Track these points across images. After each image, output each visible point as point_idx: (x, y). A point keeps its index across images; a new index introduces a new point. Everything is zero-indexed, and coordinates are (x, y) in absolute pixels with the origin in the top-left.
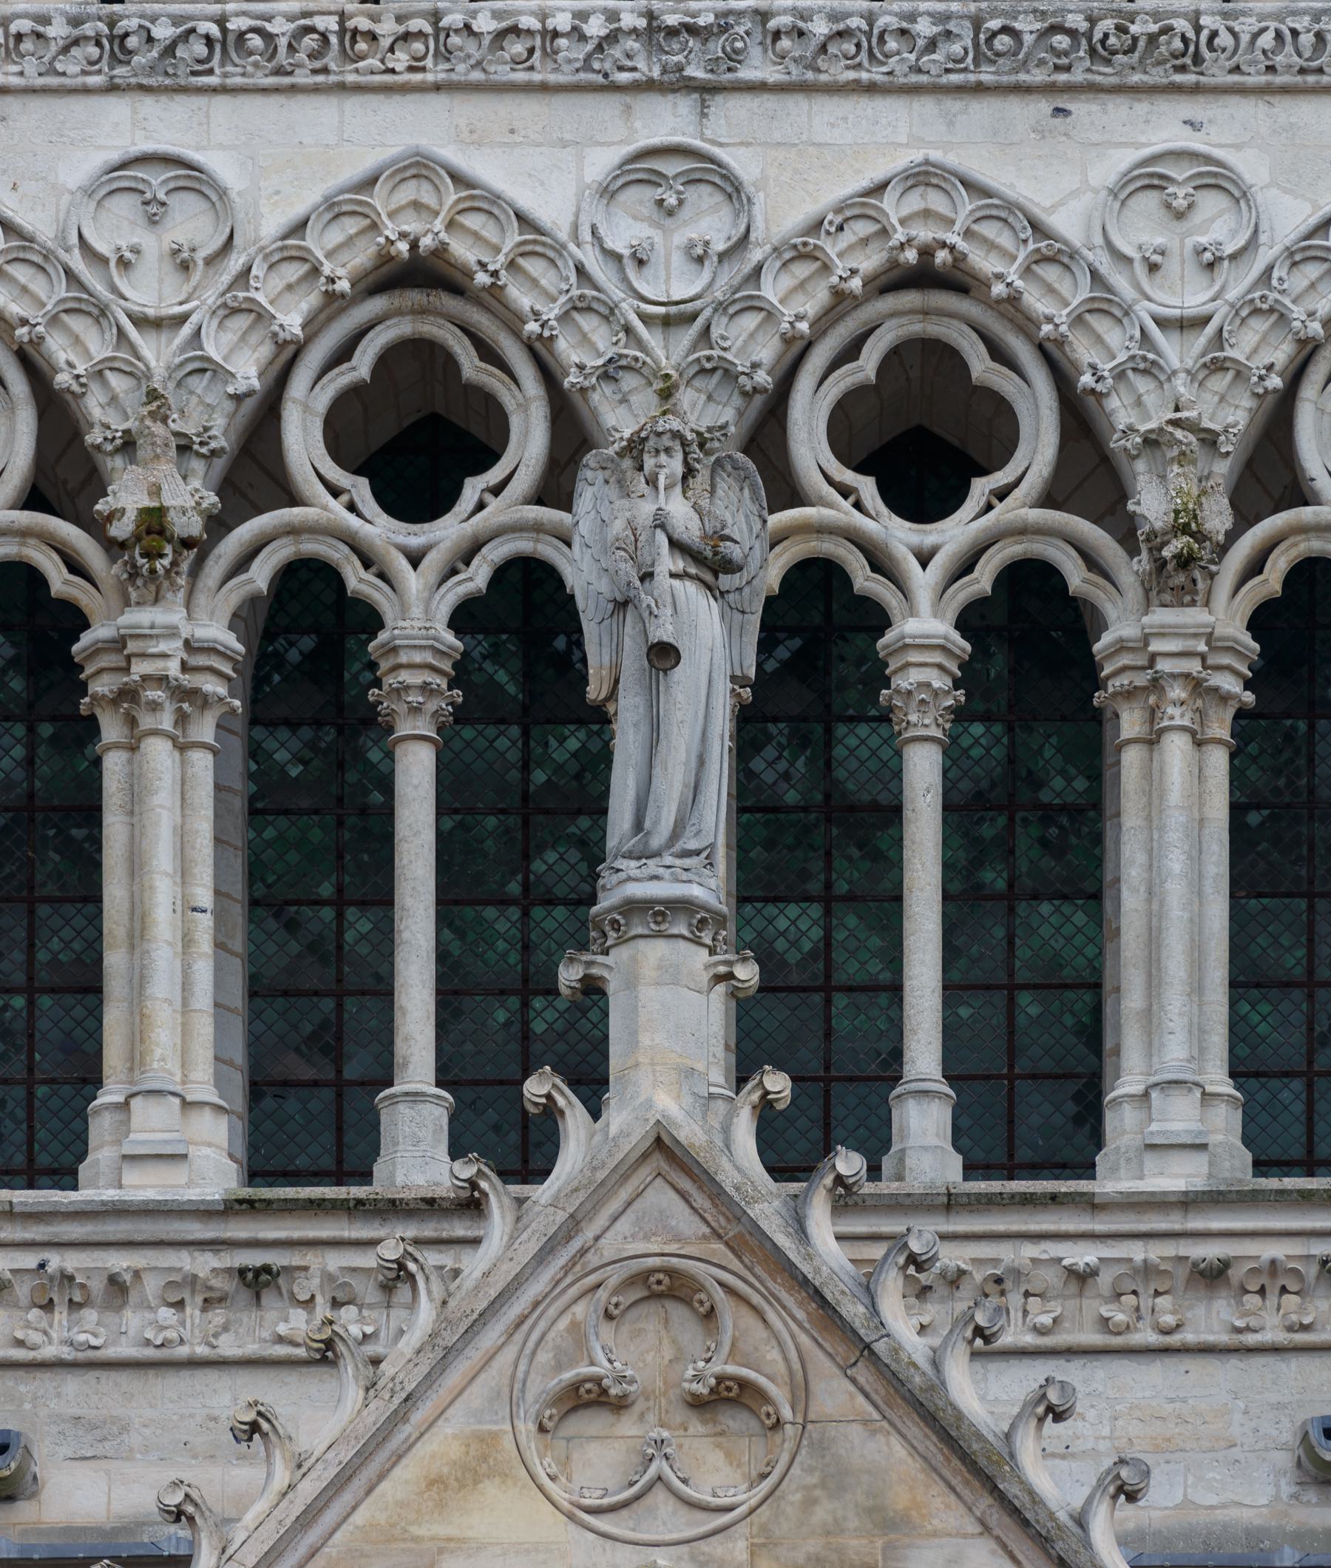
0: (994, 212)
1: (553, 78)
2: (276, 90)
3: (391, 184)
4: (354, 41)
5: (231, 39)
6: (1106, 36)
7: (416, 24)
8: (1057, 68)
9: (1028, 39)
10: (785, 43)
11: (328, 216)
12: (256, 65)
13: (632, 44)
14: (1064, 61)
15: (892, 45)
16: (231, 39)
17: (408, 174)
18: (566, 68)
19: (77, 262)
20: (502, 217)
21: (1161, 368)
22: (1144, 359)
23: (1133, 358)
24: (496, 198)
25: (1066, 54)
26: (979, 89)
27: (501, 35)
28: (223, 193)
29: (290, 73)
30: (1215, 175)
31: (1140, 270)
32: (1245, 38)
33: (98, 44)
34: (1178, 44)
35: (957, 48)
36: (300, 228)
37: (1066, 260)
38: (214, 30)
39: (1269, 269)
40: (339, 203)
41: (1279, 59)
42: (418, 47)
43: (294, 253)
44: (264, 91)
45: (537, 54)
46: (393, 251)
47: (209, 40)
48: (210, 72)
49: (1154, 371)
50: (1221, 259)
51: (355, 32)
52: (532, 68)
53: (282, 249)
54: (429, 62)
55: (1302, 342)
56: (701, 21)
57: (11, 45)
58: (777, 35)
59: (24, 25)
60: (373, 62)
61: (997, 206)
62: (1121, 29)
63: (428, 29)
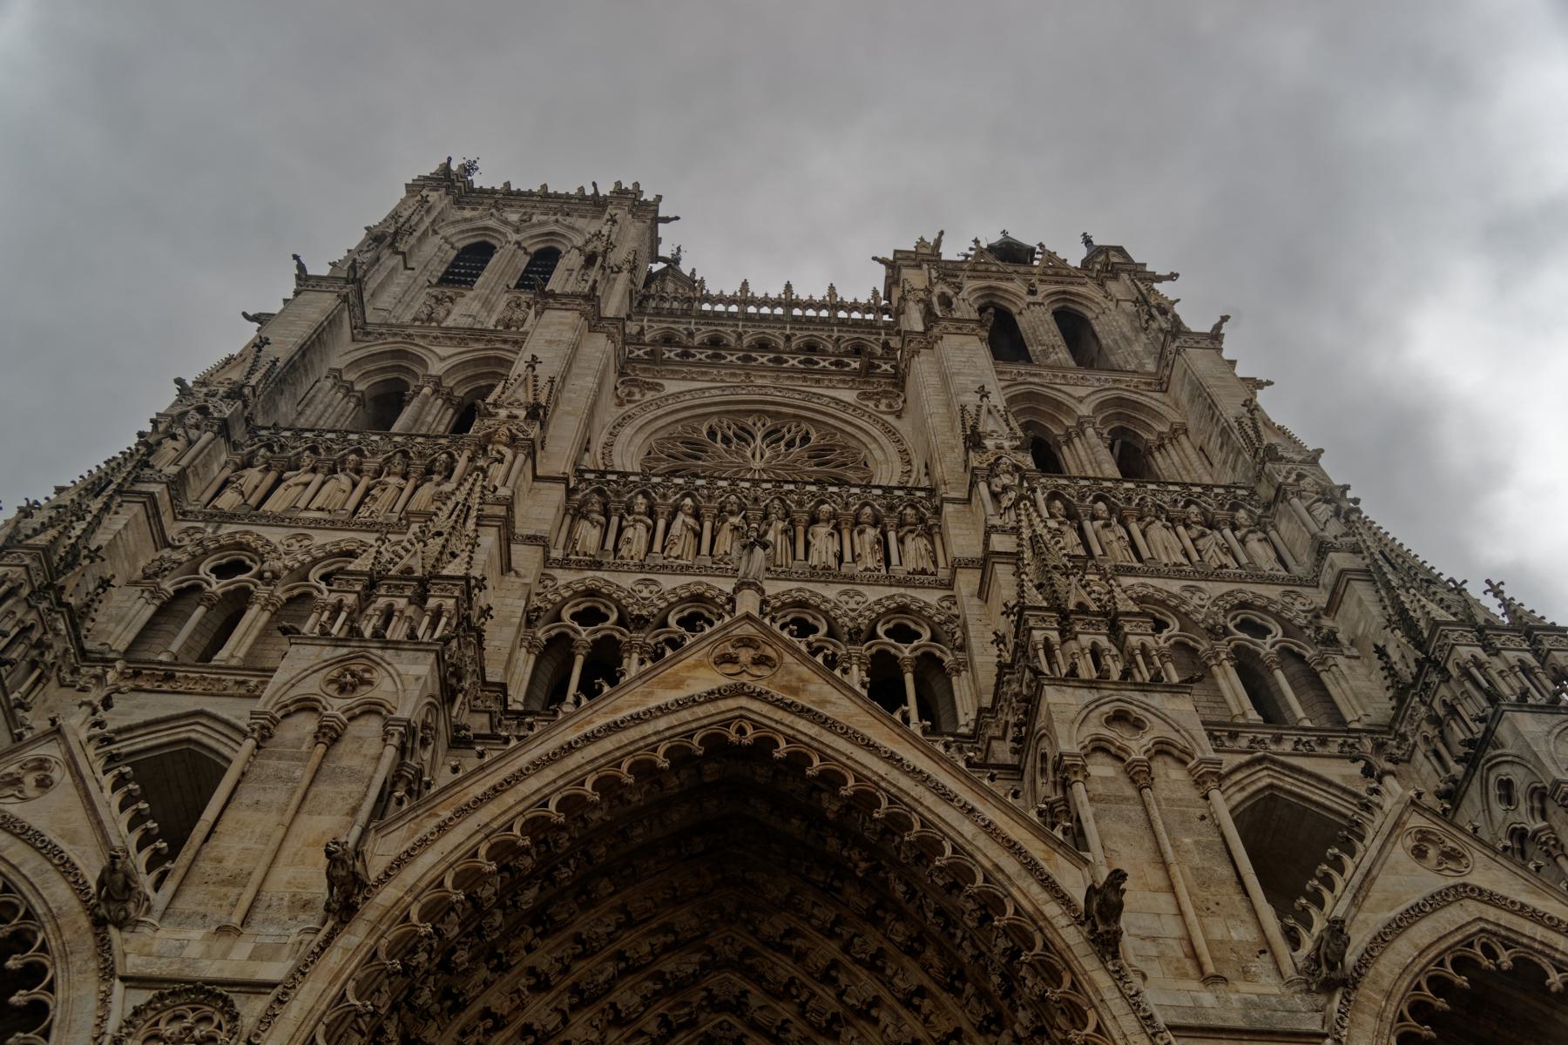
55: (878, 614)
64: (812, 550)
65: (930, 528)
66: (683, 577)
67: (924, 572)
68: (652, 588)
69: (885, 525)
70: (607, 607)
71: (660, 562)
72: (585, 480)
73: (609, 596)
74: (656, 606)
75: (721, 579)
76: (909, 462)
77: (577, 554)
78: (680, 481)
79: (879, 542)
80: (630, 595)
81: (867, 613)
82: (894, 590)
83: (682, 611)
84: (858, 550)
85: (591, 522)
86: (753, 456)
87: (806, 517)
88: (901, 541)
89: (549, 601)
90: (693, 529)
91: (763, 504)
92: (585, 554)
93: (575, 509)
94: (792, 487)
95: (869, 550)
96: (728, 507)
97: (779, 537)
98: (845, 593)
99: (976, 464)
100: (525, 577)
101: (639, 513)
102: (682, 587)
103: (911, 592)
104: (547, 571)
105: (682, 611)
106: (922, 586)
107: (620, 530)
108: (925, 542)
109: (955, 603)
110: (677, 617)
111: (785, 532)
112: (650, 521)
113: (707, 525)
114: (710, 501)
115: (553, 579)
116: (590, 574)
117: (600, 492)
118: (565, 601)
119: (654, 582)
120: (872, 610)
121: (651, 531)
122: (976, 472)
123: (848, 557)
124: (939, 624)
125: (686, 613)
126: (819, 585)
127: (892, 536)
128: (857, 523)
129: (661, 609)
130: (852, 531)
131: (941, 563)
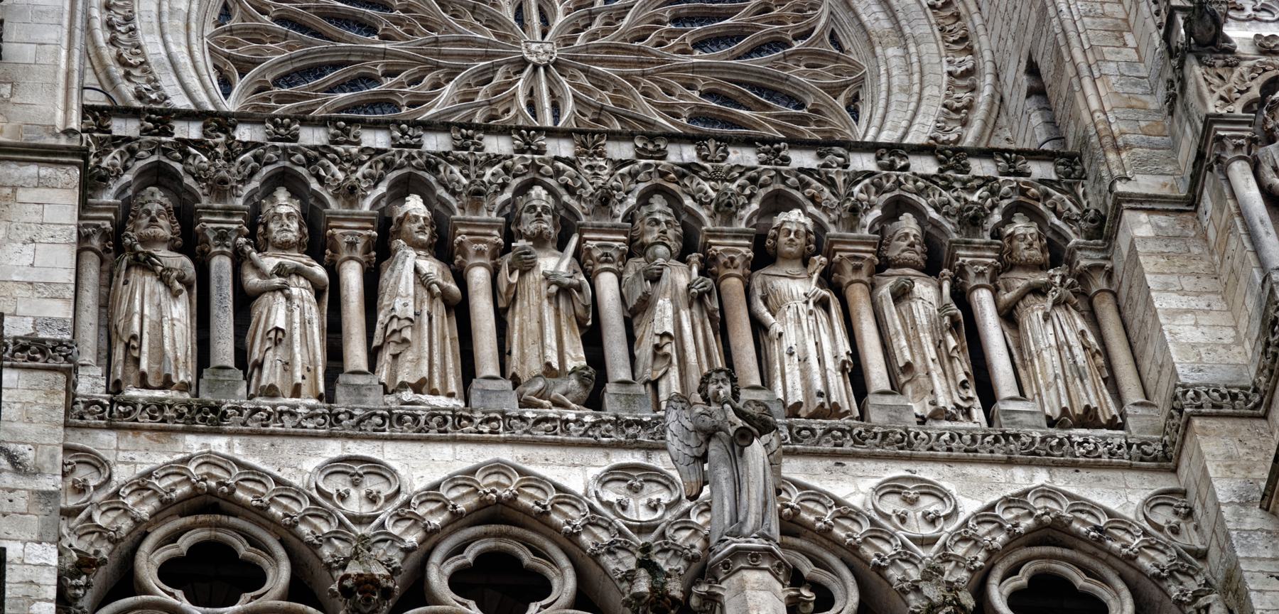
0: (811, 497)
2: (419, 440)
3: (484, 474)
4: (459, 421)
5: (395, 417)
6: (860, 432)
7: (492, 415)
8: (836, 445)
9: (819, 432)
11: (451, 485)
12: (408, 427)
14: (839, 441)
16: (395, 417)
17: (493, 471)
19: (315, 494)
20: (546, 488)
21: (916, 558)
22: (906, 553)
23: (899, 553)
25: (839, 438)
27: (538, 422)
28: (393, 472)
29: (427, 432)
30: (928, 487)
32: (934, 436)
33: (324, 418)
34: (899, 436)
36: (436, 487)
37: (854, 516)
38: (385, 413)
39: (966, 522)
40: (457, 479)
42: (495, 424)
43: (433, 497)
44: (413, 440)
45: (558, 428)
46: (488, 497)
47: (383, 417)
48: (384, 430)
49: (912, 560)
50: (939, 517)
51: (461, 417)
52: (556, 434)
53: (427, 495)
54: (501, 430)
55: (991, 552)
56: (645, 419)
57: (277, 416)
59: (285, 408)
61: (813, 494)
62: (867, 431)
63: (499, 417)
64: (776, 351)
65: (1083, 277)
66: (446, 451)
67: (1089, 418)
68: (373, 484)
69: (962, 271)
70: (254, 542)
71: (376, 401)
72: (117, 141)
73: (260, 514)
74: (395, 539)
75: (553, 453)
76: (964, 42)
77: (143, 383)
78: (377, 139)
79: (954, 326)
80: (319, 511)
81: (960, 550)
82: (1021, 479)
83: (459, 550)
84: (904, 354)
85: (163, 279)
86: (519, 14)
87: (745, 250)
88: (1009, 316)
89: (101, 532)
90: (445, 296)
91: (621, 210)
92: (167, 384)
93: (105, 235)
94: (689, 154)
95: (931, 353)
96: (529, 226)
97: (685, 315)
99: (1213, 106)
100: (38, 472)
101: (285, 246)
102: (453, 481)
103: (1064, 482)
104: (79, 440)
105: (459, 550)
106: (1091, 462)
107: (245, 302)
108: (1081, 324)
109: (1190, 514)
110: (449, 568)
111: (697, 299)
112: (320, 271)
113: (479, 277)
114: (476, 207)
115: (98, 464)
116: (193, 444)
117: (159, 176)
118: (141, 531)
119: (377, 468)
120: (976, 542)
121: (330, 295)
122: (1222, 131)
123: (877, 376)
124: (1157, 578)
125: (469, 556)
126: (819, 465)
127: (984, 302)
128: (883, 266)
129: (407, 551)
130: (872, 287)
131: (1132, 393)
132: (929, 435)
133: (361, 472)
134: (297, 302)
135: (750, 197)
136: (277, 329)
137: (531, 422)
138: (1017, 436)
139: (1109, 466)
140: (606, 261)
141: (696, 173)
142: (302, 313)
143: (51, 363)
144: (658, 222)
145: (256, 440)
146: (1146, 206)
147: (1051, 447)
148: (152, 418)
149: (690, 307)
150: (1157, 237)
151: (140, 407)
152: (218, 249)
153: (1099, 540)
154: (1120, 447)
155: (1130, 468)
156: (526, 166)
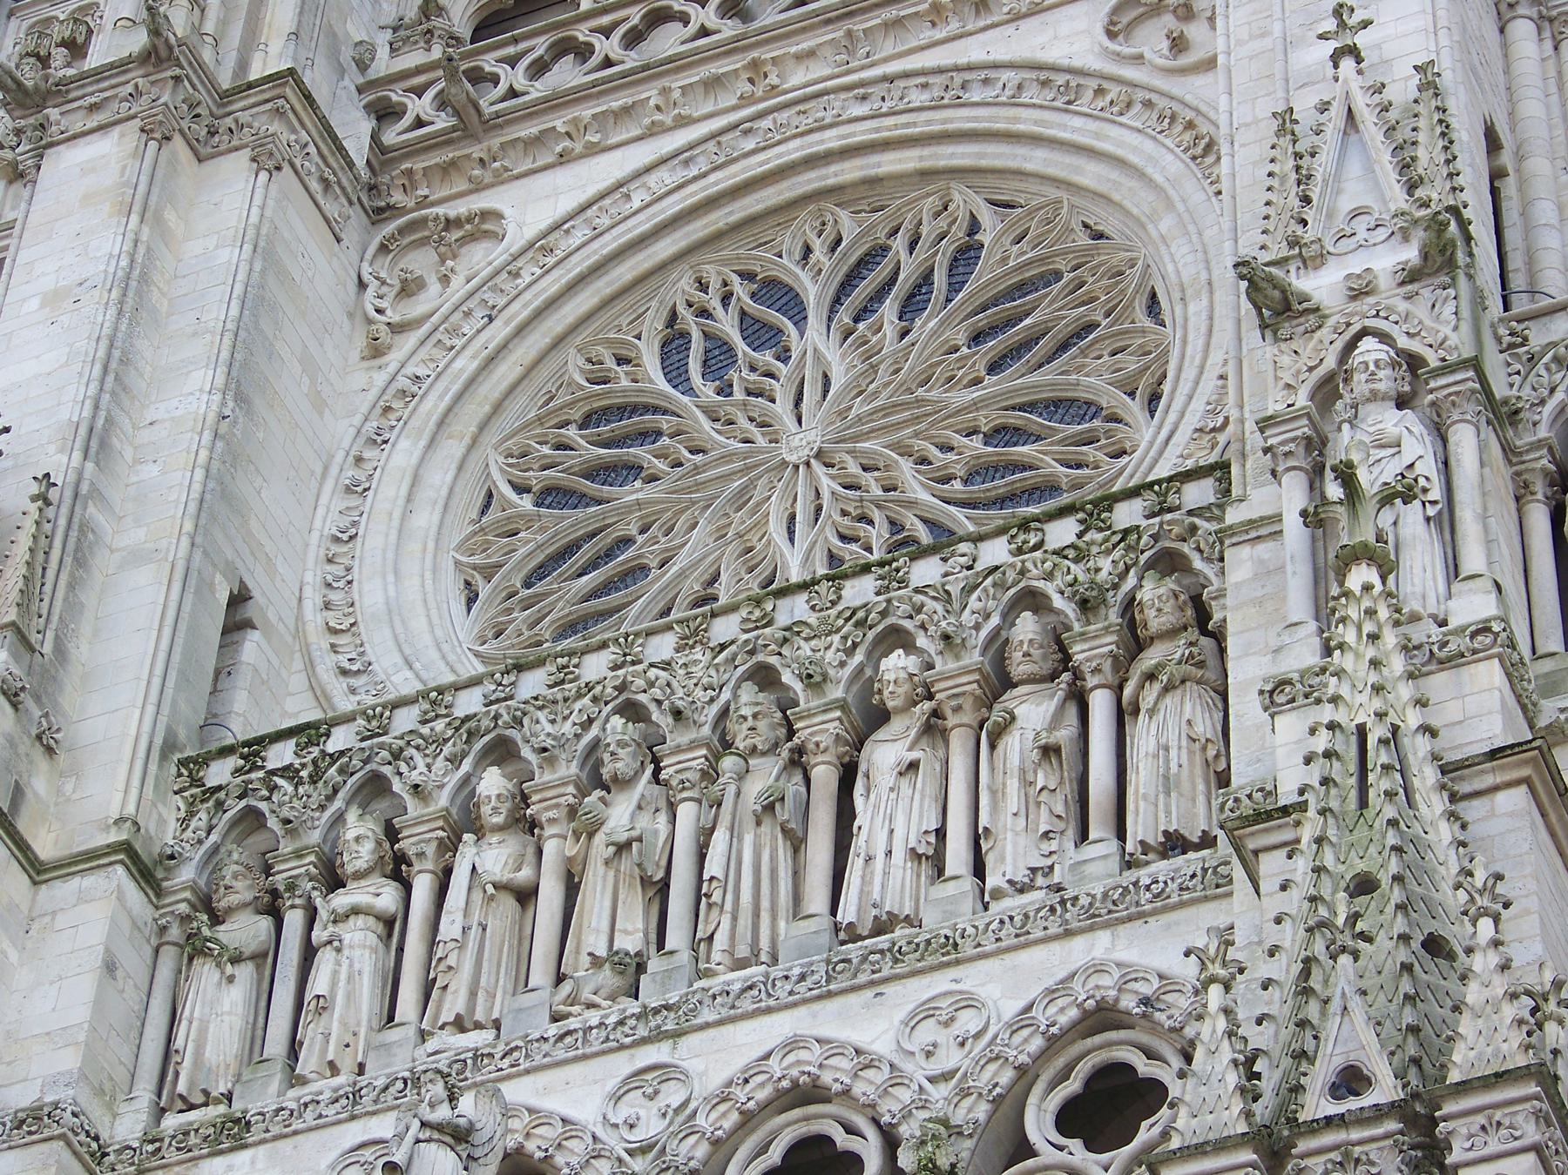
1: (588, 1050)
8: (874, 972)
10: (719, 999)
13: (632, 1022)
15: (778, 984)
18: (596, 1043)
24: (550, 1115)
26: (830, 995)
27: (561, 1038)
31: (920, 1057)
34: (943, 940)
35: (816, 977)
38: (407, 1074)
41: (1002, 934)
58: (714, 997)
60: (492, 1068)
69: (1077, 675)
98: (926, 1011)
132: (976, 927)
133: (371, 1159)
134: (346, 952)
135: (850, 652)
136: (318, 997)
137: (552, 1040)
138: (1076, 898)
139: (1182, 905)
140: (684, 789)
141: (798, 633)
142: (351, 966)
143: (47, 1133)
144: (745, 718)
145: (280, 1144)
146: (1253, 534)
147: (1114, 903)
148: (178, 1149)
149: (758, 823)
150: (1256, 576)
151: (167, 1141)
152: (288, 903)
153: (1144, 1015)
154: (1193, 876)
155: (1206, 899)
156: (615, 688)
